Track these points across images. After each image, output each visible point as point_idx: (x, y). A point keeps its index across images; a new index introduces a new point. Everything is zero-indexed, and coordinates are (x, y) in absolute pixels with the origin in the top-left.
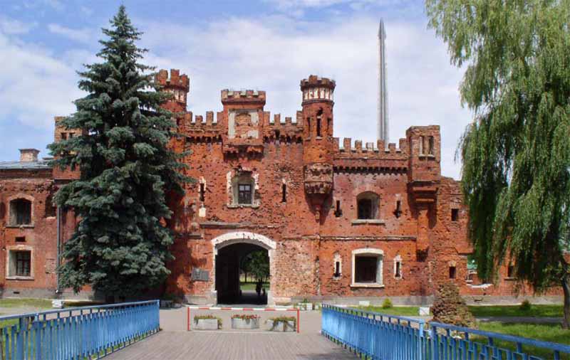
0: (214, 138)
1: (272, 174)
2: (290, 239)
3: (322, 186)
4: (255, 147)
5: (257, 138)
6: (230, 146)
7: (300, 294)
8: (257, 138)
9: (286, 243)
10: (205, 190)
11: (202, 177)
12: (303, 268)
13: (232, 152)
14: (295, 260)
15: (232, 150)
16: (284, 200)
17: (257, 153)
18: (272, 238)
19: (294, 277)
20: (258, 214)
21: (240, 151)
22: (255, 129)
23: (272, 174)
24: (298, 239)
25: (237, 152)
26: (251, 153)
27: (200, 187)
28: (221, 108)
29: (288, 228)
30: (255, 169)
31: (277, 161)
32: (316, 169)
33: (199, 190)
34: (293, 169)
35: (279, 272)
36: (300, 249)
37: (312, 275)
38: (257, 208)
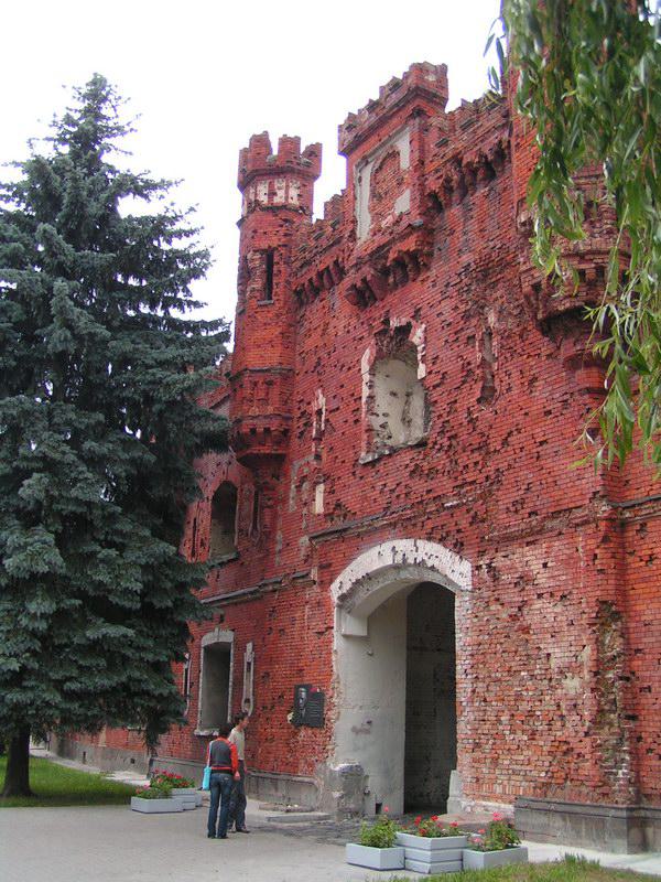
2: (508, 539)
7: (547, 785)
9: (499, 562)
12: (554, 663)
14: (526, 630)
17: (413, 256)
18: (458, 548)
19: (524, 706)
24: (530, 537)
29: (505, 498)
30: (416, 315)
31: (466, 258)
35: (481, 686)
36: (543, 580)
37: (588, 694)
38: (422, 444)
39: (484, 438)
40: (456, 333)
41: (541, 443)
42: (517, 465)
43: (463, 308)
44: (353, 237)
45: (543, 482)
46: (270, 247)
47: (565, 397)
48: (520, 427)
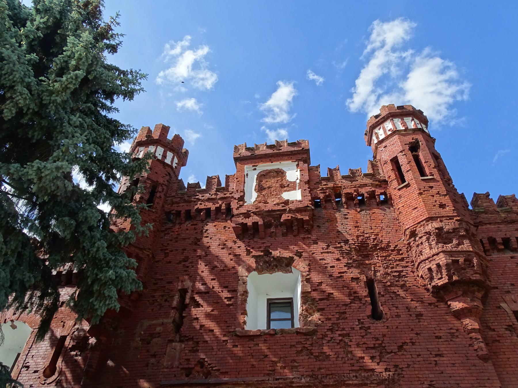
0: (218, 209)
1: (338, 260)
3: (468, 261)
4: (299, 210)
5: (299, 198)
6: (247, 215)
8: (299, 198)
10: (187, 301)
11: (186, 277)
13: (250, 224)
15: (249, 222)
16: (376, 315)
20: (316, 351)
21: (267, 225)
22: (294, 189)
23: (338, 260)
25: (261, 222)
26: (289, 224)
27: (177, 298)
28: (231, 169)
32: (440, 229)
33: (175, 303)
34: (382, 249)
39: (380, 342)
40: (339, 273)
41: (436, 355)
42: (415, 366)
43: (345, 261)
44: (242, 199)
45: (447, 382)
46: (157, 181)
47: (452, 331)
48: (414, 341)
